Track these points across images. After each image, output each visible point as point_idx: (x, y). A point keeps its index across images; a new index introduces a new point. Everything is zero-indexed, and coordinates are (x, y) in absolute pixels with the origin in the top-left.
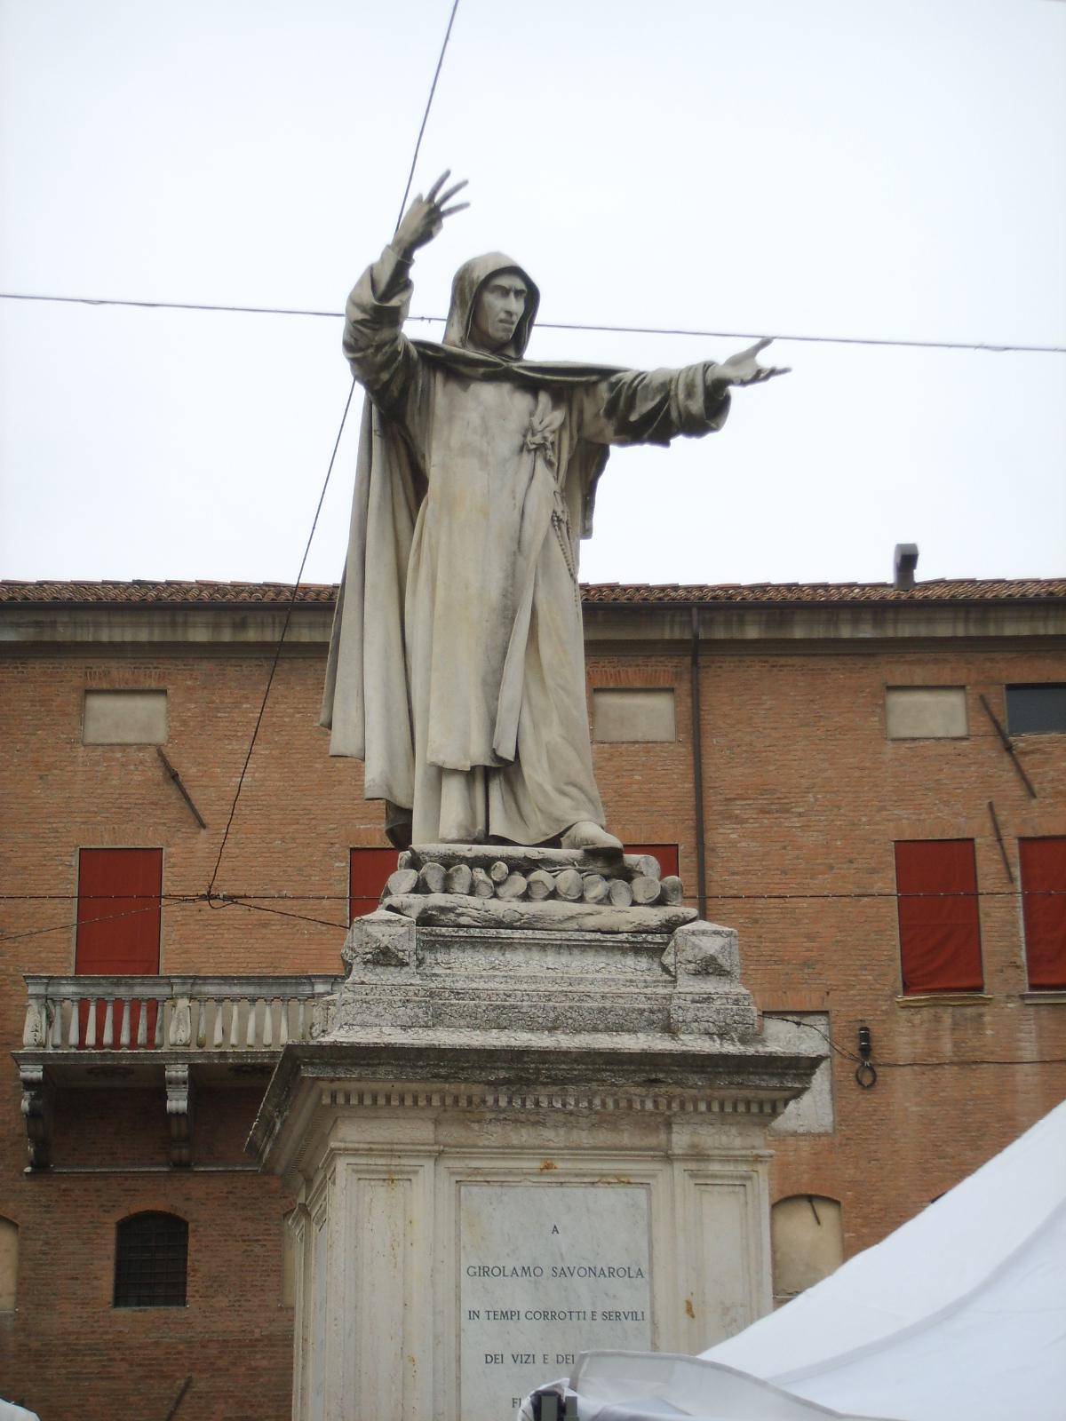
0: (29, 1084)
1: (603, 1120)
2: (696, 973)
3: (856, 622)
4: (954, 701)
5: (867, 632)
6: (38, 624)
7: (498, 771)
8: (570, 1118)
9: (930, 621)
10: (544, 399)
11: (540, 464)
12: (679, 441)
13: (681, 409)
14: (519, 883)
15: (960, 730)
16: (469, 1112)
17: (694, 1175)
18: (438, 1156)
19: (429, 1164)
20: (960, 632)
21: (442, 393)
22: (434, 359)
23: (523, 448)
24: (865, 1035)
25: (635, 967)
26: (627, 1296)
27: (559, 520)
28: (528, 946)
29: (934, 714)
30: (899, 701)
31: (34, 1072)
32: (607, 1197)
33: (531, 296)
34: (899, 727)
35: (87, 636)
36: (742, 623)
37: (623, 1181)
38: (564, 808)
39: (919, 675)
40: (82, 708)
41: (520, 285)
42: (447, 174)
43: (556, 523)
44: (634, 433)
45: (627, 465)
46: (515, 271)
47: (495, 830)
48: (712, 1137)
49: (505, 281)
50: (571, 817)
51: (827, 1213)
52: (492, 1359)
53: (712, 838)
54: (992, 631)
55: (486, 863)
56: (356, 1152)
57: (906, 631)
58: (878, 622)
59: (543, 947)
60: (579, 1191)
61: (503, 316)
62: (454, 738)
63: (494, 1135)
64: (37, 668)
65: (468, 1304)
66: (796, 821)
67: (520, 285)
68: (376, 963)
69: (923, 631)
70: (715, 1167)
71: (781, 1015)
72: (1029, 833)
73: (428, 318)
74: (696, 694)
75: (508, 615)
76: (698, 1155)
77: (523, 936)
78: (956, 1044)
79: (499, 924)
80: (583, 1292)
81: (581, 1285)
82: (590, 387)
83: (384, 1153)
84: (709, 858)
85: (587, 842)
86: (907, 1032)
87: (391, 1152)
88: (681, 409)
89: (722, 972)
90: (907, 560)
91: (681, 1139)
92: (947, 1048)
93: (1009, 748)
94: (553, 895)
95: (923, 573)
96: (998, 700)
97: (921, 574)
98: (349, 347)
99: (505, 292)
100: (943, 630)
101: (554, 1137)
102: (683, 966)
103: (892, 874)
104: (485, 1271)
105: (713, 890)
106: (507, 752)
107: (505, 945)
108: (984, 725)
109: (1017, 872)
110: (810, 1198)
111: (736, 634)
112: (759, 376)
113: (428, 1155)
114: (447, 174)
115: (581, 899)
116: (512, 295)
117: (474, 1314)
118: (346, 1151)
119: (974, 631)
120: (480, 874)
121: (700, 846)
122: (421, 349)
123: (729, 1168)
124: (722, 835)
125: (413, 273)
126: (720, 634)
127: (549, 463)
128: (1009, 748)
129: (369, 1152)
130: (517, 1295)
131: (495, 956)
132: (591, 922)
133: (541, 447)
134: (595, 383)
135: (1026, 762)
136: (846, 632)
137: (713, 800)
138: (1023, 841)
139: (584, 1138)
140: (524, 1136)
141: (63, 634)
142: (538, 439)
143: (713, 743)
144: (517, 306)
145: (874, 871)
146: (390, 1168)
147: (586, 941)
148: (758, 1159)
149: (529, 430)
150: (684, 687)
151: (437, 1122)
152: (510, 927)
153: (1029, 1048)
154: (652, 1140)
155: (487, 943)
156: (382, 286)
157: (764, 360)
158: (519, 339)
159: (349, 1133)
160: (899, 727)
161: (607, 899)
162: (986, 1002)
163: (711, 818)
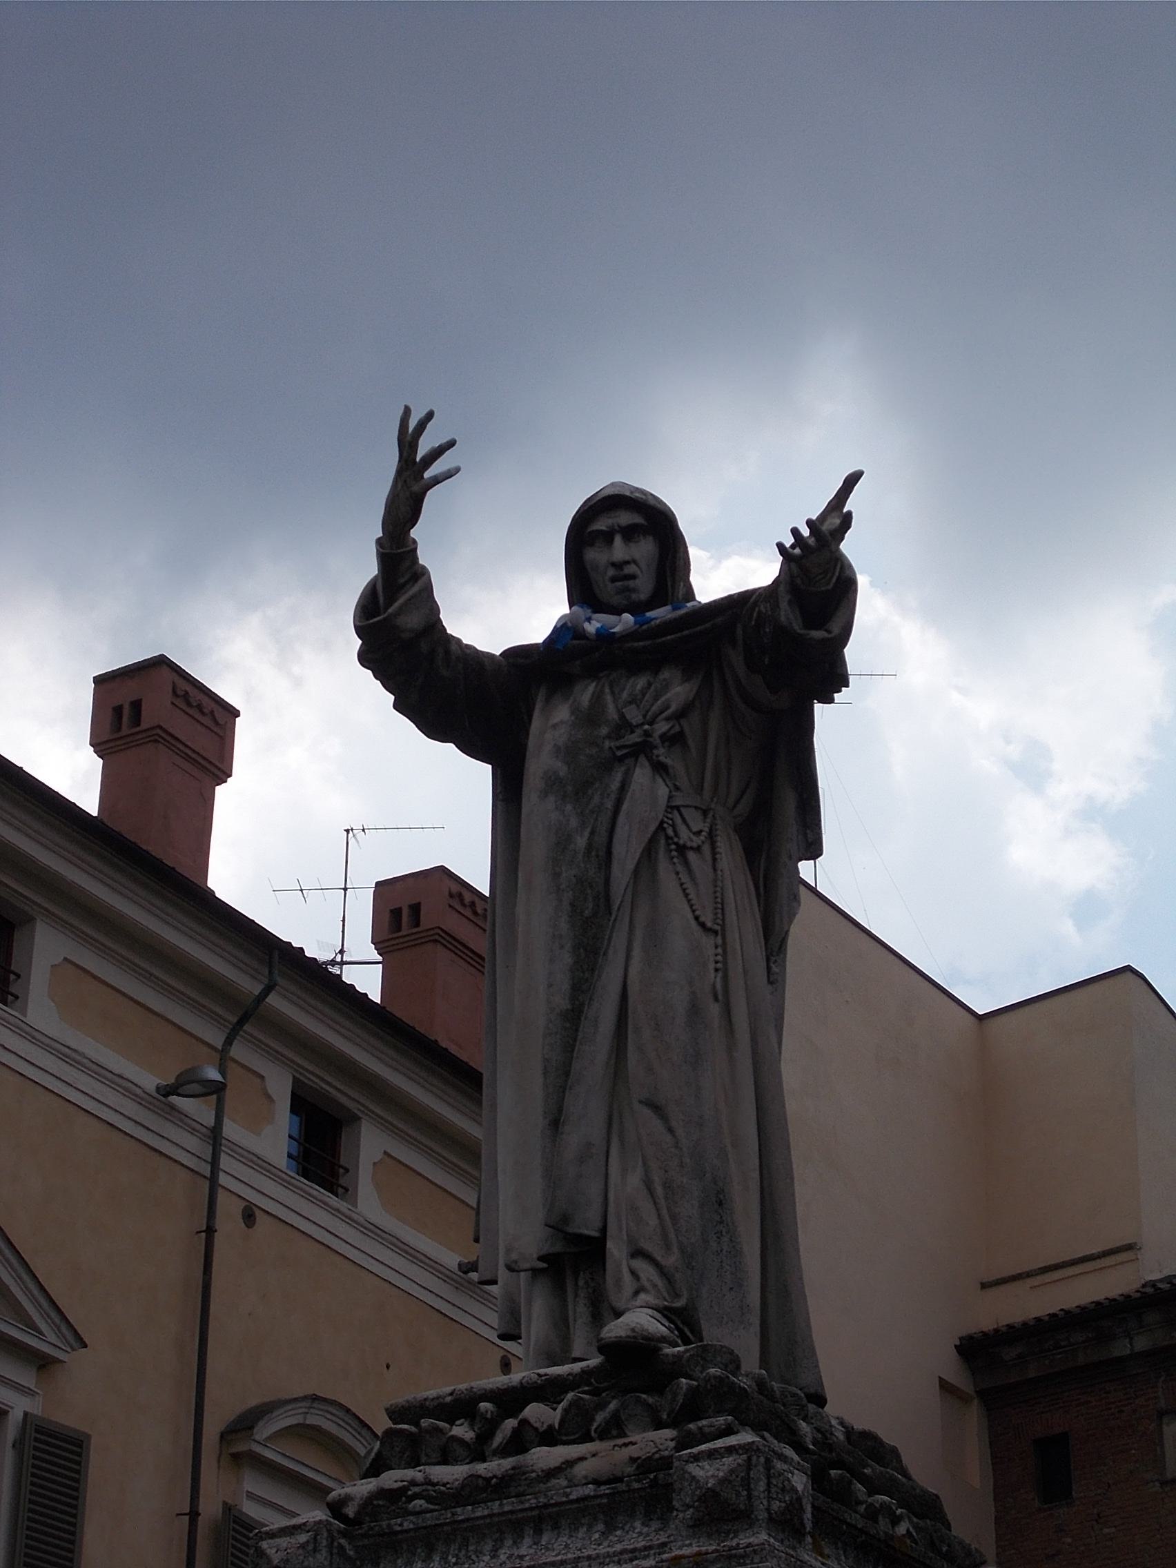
27: (682, 849)
41: (626, 518)
42: (407, 411)
49: (601, 525)
61: (611, 572)
67: (626, 518)
77: (486, 1512)
94: (549, 1438)
99: (607, 537)
102: (681, 1515)
114: (407, 411)
115: (586, 1438)
116: (618, 540)
127: (660, 768)
132: (580, 1470)
142: (635, 738)
144: (645, 549)
147: (572, 1502)
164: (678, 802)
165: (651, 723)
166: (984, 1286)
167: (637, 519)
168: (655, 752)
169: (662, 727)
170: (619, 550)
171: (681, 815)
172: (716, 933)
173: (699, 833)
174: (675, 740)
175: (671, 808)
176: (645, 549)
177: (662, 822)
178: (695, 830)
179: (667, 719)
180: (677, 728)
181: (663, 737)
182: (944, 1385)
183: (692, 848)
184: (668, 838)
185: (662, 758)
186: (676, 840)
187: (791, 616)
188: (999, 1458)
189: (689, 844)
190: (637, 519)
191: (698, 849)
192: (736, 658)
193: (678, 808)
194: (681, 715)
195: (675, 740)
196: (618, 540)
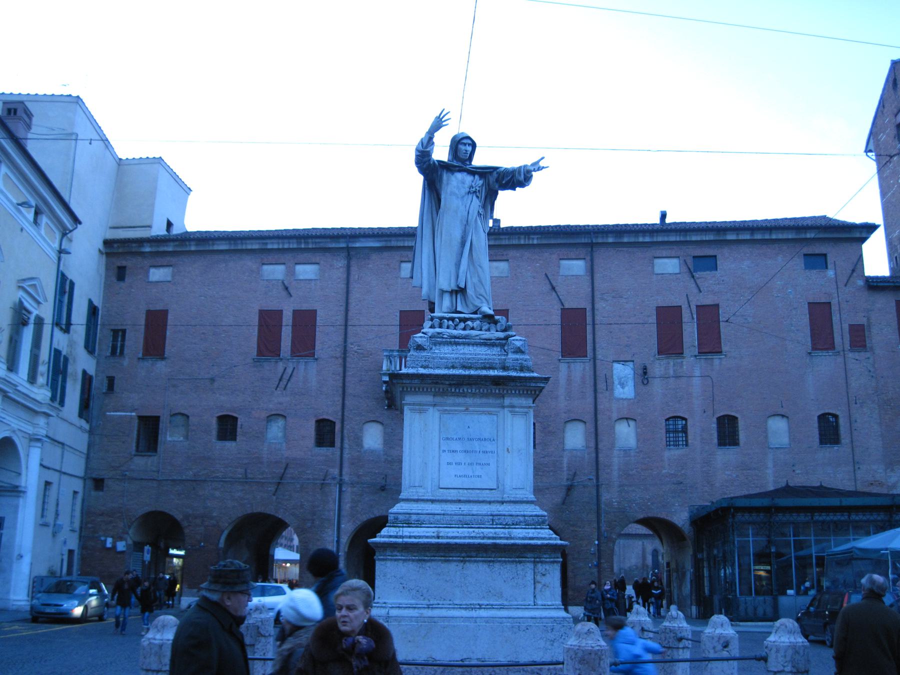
0: (385, 382)
1: (483, 395)
2: (514, 352)
3: (644, 236)
4: (675, 261)
5: (647, 239)
6: (386, 241)
7: (460, 291)
8: (474, 395)
9: (668, 236)
10: (477, 177)
11: (474, 197)
12: (517, 189)
13: (516, 179)
14: (462, 325)
15: (677, 271)
16: (443, 394)
17: (511, 412)
18: (435, 405)
19: (431, 408)
20: (678, 239)
21: (445, 176)
22: (442, 165)
23: (469, 192)
24: (645, 368)
25: (496, 350)
26: (489, 447)
28: (464, 344)
29: (669, 266)
30: (657, 261)
31: (386, 379)
32: (484, 418)
33: (474, 145)
34: (657, 270)
35: (401, 244)
36: (607, 237)
37: (490, 413)
38: (477, 303)
39: (664, 253)
40: (400, 266)
41: (470, 142)
44: (505, 187)
45: (504, 197)
46: (468, 138)
47: (459, 309)
48: (516, 401)
49: (465, 141)
50: (480, 305)
51: (632, 423)
52: (449, 464)
53: (597, 306)
54: (688, 239)
55: (453, 319)
56: (410, 404)
57: (660, 239)
58: (651, 236)
59: (469, 344)
60: (476, 416)
62: (445, 282)
63: (451, 400)
64: (386, 254)
65: (443, 448)
66: (625, 301)
67: (470, 142)
68: (417, 349)
69: (666, 239)
70: (517, 409)
71: (618, 362)
72: (699, 304)
73: (441, 153)
74: (592, 260)
75: (463, 244)
76: (513, 406)
78: (674, 371)
79: (455, 337)
80: (476, 445)
81: (476, 443)
82: (491, 173)
83: (418, 405)
84: (596, 312)
85: (484, 312)
86: (659, 367)
87: (420, 405)
88: (516, 179)
89: (522, 352)
90: (663, 216)
91: (507, 401)
92: (671, 372)
93: (693, 277)
94: (473, 329)
95: (668, 220)
96: (690, 261)
97: (668, 220)
98: (417, 163)
99: (465, 144)
100: (672, 238)
101: (469, 401)
103: (655, 317)
104: (447, 439)
105: (597, 322)
106: (462, 286)
107: (457, 344)
108: (685, 269)
109: (695, 316)
110: (627, 419)
111: (605, 241)
112: (540, 169)
113: (431, 405)
115: (481, 330)
117: (444, 451)
118: (407, 404)
119: (682, 239)
120: (450, 323)
121: (593, 309)
123: (521, 410)
124: (599, 305)
125: (434, 140)
126: (600, 240)
127: (477, 197)
128: (693, 277)
129: (414, 404)
130: (456, 446)
131: (454, 347)
133: (475, 192)
135: (698, 281)
136: (641, 239)
137: (597, 294)
138: (697, 306)
139: (478, 401)
140: (461, 400)
141: (394, 243)
143: (597, 276)
144: (469, 149)
145: (649, 316)
146: (421, 409)
148: (530, 407)
149: (472, 187)
150: (588, 258)
151: (434, 396)
152: (458, 338)
153: (697, 373)
154: (498, 401)
155: (450, 343)
156: (425, 144)
157: (541, 164)
158: (471, 158)
159: (409, 399)
160: (657, 270)
161: (489, 330)
162: (684, 358)
163: (596, 300)
166: (111, 228)
182: (100, 250)
188: (107, 269)
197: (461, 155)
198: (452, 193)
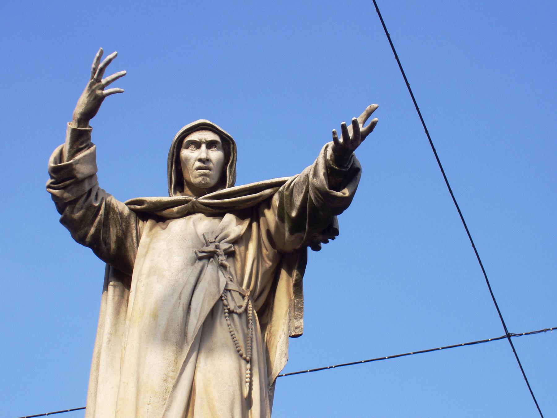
27: (231, 312)
33: (227, 144)
41: (210, 136)
43: (227, 314)
61: (198, 164)
67: (210, 136)
99: (197, 145)
112: (360, 137)
116: (204, 146)
122: (132, 207)
127: (223, 267)
133: (211, 255)
134: (271, 196)
164: (230, 287)
165: (219, 242)
167: (216, 138)
168: (220, 258)
169: (224, 246)
170: (203, 152)
171: (231, 295)
172: (248, 362)
173: (240, 307)
174: (230, 254)
175: (226, 290)
176: (216, 155)
177: (221, 297)
178: (238, 304)
179: (228, 242)
180: (233, 249)
181: (225, 250)
183: (236, 313)
184: (224, 305)
185: (224, 262)
186: (228, 307)
187: (325, 182)
189: (235, 311)
190: (216, 138)
191: (240, 315)
192: (271, 216)
193: (230, 291)
194: (236, 241)
195: (230, 254)
196: (204, 146)
197: (194, 176)
198: (153, 271)
